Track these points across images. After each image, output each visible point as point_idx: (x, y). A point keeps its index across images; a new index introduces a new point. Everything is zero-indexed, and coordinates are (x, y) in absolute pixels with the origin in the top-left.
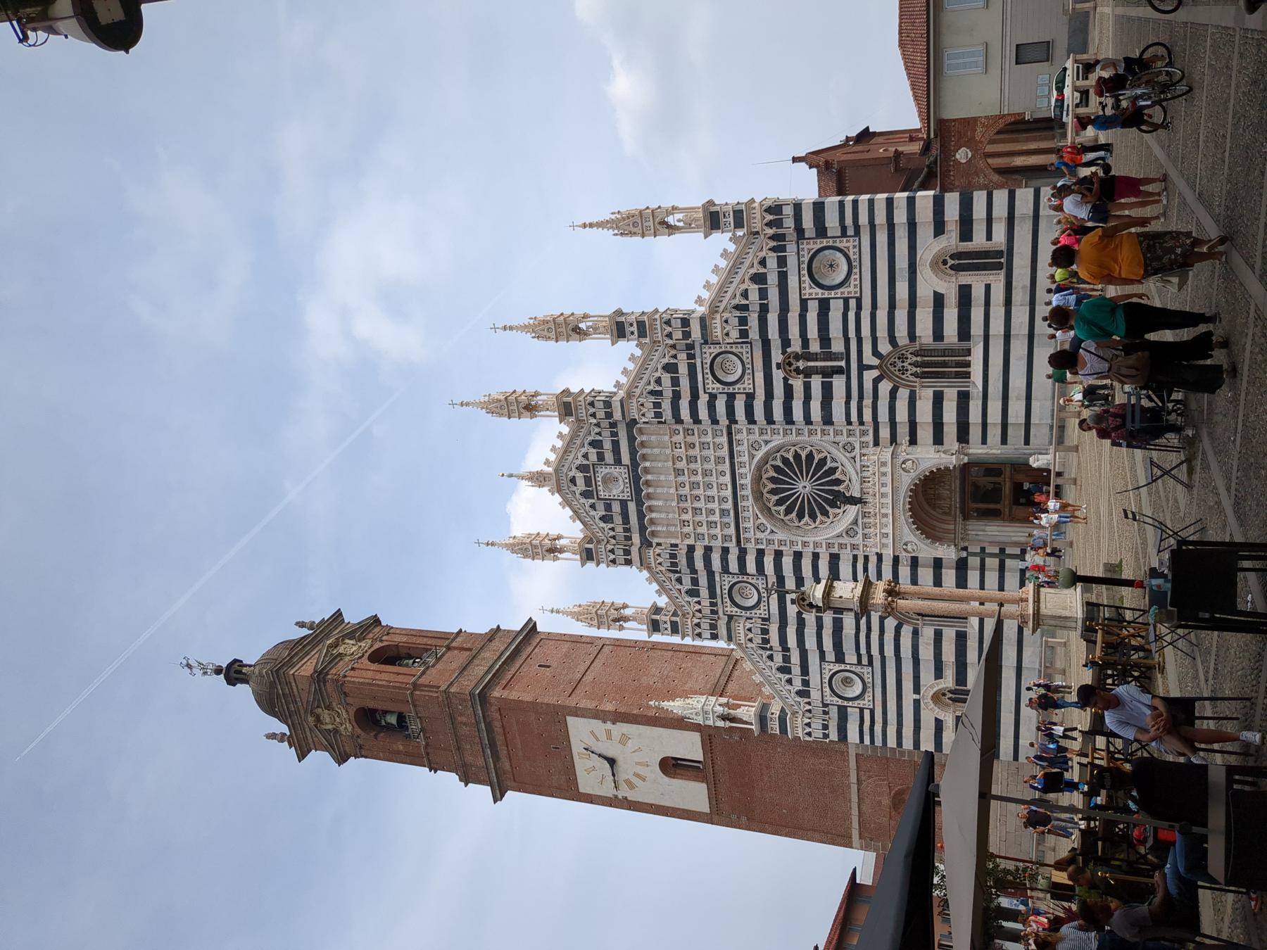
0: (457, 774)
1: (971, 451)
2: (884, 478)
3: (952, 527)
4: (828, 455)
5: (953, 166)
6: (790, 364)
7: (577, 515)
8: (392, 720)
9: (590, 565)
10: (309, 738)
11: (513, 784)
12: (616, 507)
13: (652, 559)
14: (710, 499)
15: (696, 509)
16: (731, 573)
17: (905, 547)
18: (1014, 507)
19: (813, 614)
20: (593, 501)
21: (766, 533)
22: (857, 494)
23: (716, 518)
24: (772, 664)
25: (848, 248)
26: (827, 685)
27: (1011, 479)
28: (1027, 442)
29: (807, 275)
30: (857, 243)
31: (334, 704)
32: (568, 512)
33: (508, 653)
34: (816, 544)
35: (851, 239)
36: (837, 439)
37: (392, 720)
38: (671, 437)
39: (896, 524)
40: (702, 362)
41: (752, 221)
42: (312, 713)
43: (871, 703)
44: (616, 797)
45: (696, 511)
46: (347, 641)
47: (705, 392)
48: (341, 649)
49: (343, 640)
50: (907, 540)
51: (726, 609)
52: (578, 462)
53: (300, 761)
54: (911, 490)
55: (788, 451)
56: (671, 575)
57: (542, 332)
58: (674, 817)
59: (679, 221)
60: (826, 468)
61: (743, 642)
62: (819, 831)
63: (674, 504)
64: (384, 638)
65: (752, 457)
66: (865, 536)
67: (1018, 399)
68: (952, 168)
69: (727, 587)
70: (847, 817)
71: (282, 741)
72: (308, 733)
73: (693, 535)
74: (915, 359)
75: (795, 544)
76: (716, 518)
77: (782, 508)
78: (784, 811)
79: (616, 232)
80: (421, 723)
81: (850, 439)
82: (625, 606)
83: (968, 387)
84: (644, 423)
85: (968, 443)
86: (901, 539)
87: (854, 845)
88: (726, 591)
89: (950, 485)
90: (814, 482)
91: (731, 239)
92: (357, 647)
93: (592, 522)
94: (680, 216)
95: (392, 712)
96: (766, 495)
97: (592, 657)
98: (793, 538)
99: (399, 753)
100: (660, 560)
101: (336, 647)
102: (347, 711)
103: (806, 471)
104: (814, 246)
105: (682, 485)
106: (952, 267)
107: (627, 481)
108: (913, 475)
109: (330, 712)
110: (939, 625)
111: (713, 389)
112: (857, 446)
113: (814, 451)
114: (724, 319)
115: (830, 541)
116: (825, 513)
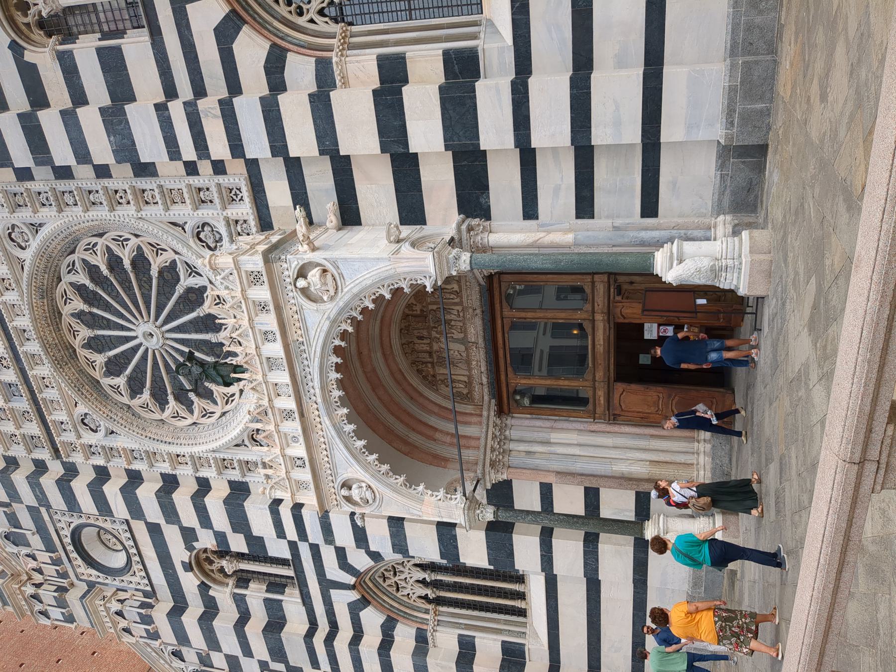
1: (494, 239)
4: (176, 257)
17: (344, 492)
18: (620, 387)
19: (228, 590)
27: (609, 313)
28: (650, 207)
39: (314, 437)
50: (345, 476)
54: (337, 351)
55: (91, 248)
60: (179, 290)
67: (621, 63)
69: (66, 533)
77: (121, 381)
83: (475, 37)
85: (488, 217)
86: (334, 474)
89: (464, 330)
96: (82, 353)
98: (151, 446)
103: (143, 295)
108: (331, 309)
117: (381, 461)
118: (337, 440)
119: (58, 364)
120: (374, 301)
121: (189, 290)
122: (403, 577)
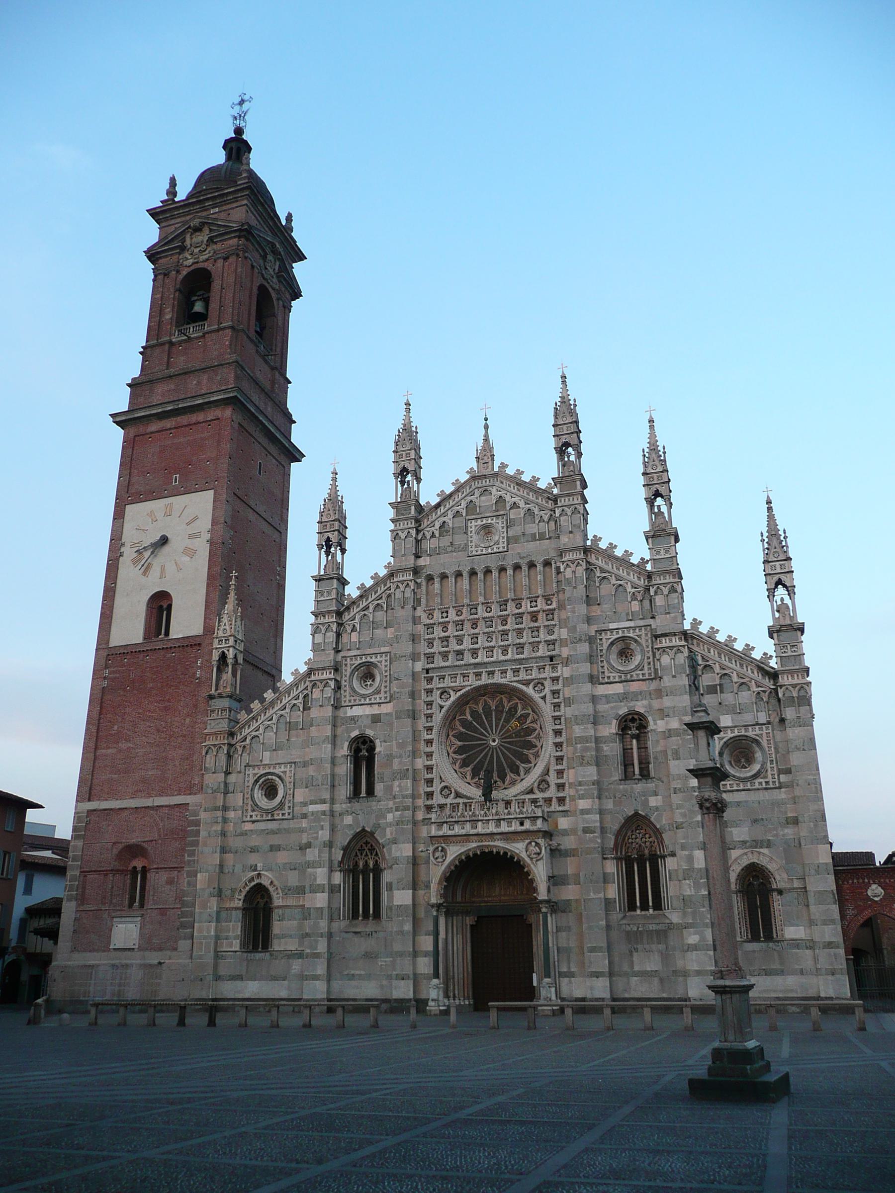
0: (140, 375)
2: (518, 823)
3: (459, 899)
4: (533, 765)
5: (864, 882)
6: (633, 720)
7: (446, 498)
8: (198, 307)
9: (391, 513)
10: (173, 222)
11: (132, 435)
12: (459, 540)
13: (401, 579)
14: (475, 638)
15: (462, 624)
16: (391, 663)
17: (440, 848)
20: (464, 515)
21: (439, 701)
22: (495, 794)
23: (454, 646)
24: (288, 710)
25: (765, 777)
26: (267, 771)
29: (733, 735)
30: (771, 786)
31: (215, 247)
32: (449, 489)
33: (272, 430)
34: (429, 755)
35: (776, 780)
36: (553, 774)
37: (198, 307)
38: (543, 596)
40: (630, 627)
41: (789, 676)
42: (203, 224)
43: (248, 818)
44: (123, 545)
45: (460, 624)
46: (278, 263)
47: (596, 631)
48: (270, 257)
49: (279, 259)
50: (448, 850)
51: (348, 659)
52: (508, 498)
53: (147, 211)
54: (505, 853)
56: (384, 599)
57: (652, 460)
58: (102, 608)
59: (782, 600)
60: (518, 763)
61: (313, 678)
62: (94, 766)
63: (466, 601)
64: (281, 302)
65: (527, 683)
66: (442, 807)
68: (861, 881)
70: (112, 794)
71: (168, 193)
72: (179, 220)
73: (432, 622)
74: (646, 851)
75: (429, 732)
76: (454, 646)
78: (116, 727)
79: (766, 534)
80: (196, 338)
81: (553, 788)
82: (343, 551)
84: (558, 568)
87: (79, 803)
88: (369, 659)
90: (501, 750)
91: (765, 654)
92: (273, 273)
93: (439, 513)
94: (787, 600)
95: (207, 307)
97: (270, 520)
99: (161, 313)
100: (402, 587)
101: (272, 252)
102: (207, 260)
104: (765, 741)
105: (488, 609)
106: (750, 884)
107: (490, 551)
108: (524, 855)
109: (205, 242)
110: (344, 888)
111: (601, 639)
112: (547, 795)
113: (537, 749)
114: (681, 649)
115: (435, 767)
116: (465, 764)
117: (456, 866)
118: (466, 849)
119: (477, 689)
120: (527, 872)
121: (518, 767)
122: (369, 854)
